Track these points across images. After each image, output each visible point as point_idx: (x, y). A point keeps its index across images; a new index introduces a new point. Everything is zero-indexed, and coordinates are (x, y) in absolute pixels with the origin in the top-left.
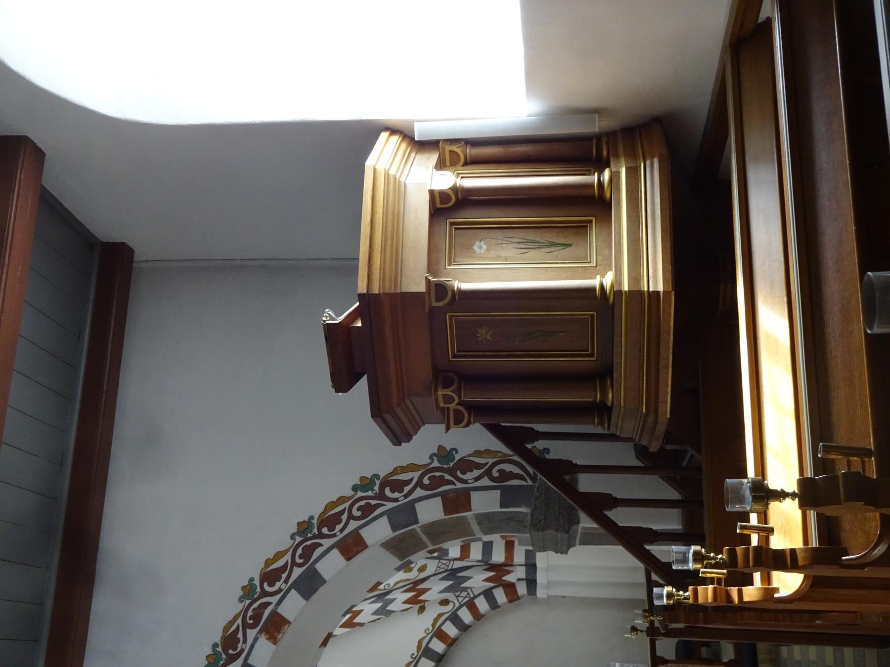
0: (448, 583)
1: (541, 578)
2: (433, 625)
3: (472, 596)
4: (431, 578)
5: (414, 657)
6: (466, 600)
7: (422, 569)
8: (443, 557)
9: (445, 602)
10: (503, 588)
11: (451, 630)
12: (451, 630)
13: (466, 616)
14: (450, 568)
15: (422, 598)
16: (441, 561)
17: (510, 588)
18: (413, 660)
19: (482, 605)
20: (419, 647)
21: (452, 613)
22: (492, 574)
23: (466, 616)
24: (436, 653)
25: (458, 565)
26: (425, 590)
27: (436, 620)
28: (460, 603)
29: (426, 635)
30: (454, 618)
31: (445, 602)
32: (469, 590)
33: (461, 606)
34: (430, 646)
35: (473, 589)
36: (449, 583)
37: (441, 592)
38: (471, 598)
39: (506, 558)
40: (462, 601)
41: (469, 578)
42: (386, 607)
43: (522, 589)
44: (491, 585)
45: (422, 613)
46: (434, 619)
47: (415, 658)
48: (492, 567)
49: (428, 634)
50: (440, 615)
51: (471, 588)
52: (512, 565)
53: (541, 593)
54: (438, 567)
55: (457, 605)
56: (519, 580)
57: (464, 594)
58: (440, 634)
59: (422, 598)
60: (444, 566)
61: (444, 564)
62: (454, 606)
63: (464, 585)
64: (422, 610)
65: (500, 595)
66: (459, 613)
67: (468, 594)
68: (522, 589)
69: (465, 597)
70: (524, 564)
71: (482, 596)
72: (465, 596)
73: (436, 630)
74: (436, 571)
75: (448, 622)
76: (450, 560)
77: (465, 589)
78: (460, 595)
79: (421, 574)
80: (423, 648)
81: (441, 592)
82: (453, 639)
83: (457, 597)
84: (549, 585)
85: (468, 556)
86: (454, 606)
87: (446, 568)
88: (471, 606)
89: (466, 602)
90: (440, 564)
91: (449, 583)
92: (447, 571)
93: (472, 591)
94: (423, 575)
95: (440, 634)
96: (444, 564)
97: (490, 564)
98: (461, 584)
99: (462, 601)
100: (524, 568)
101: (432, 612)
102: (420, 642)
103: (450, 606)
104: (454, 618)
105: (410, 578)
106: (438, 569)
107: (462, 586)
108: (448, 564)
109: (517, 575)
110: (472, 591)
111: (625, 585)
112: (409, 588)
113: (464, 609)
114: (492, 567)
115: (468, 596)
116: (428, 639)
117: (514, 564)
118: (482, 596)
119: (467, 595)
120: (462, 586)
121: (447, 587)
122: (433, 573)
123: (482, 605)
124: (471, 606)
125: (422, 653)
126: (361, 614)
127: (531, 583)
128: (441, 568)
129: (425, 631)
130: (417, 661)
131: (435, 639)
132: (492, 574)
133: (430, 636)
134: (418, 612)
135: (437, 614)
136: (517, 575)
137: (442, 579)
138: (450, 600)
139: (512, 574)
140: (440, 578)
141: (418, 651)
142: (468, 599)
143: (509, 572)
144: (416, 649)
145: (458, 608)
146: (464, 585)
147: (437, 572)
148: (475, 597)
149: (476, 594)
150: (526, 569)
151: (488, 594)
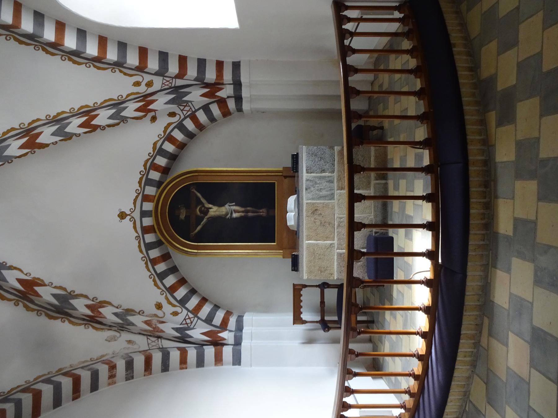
0: (172, 96)
1: (245, 93)
2: (165, 132)
3: (194, 110)
4: (158, 93)
5: (150, 155)
6: (189, 113)
7: (149, 84)
8: (183, 104)
9: (172, 114)
10: (217, 103)
11: (179, 136)
12: (179, 136)
13: (190, 125)
14: (173, 85)
15: (151, 107)
16: (164, 78)
17: (222, 102)
18: (150, 157)
19: (202, 117)
20: (154, 148)
21: (179, 122)
22: (207, 90)
23: (190, 125)
24: (168, 152)
25: (179, 82)
26: (153, 102)
27: (166, 128)
28: (184, 116)
29: (159, 139)
30: (181, 127)
31: (172, 114)
32: (190, 104)
33: (185, 118)
34: (163, 147)
35: (192, 103)
36: (172, 96)
37: (166, 103)
38: (193, 111)
39: (217, 76)
40: (186, 115)
41: (189, 93)
42: (121, 113)
43: (231, 104)
44: (206, 100)
45: (154, 122)
46: (164, 127)
47: (152, 156)
48: (207, 85)
49: (161, 138)
50: (169, 125)
51: (191, 102)
52: (223, 84)
53: (246, 106)
54: (163, 84)
55: (182, 117)
56: (228, 97)
57: (187, 108)
58: (170, 139)
59: (151, 107)
60: (168, 83)
61: (168, 81)
62: (180, 117)
63: (184, 99)
64: (154, 119)
65: (215, 110)
66: (184, 123)
67: (191, 108)
68: (231, 104)
69: (189, 111)
70: (232, 82)
71: (201, 110)
72: (188, 110)
73: (167, 135)
74: (162, 87)
75: (176, 130)
76: (172, 78)
77: (187, 102)
78: (184, 109)
79: (149, 88)
80: (157, 148)
81: (166, 103)
82: (181, 142)
83: (182, 110)
84: (251, 100)
85: (185, 74)
86: (180, 117)
87: (170, 85)
88: (193, 118)
89: (190, 114)
90: (164, 81)
91: (172, 96)
92: (171, 88)
93: (192, 104)
94: (151, 90)
95: (170, 139)
96: (168, 81)
97: (206, 83)
98: (183, 98)
99: (186, 115)
100: (232, 86)
101: (163, 121)
102: (155, 144)
103: (177, 117)
104: (181, 127)
105: (140, 92)
106: (163, 85)
107: (183, 99)
108: (171, 81)
109: (227, 92)
110: (192, 104)
111: (308, 97)
112: (140, 100)
113: (188, 119)
114: (207, 85)
115: (191, 110)
116: (162, 142)
117: (225, 83)
118: (201, 110)
119: (190, 110)
120: (183, 99)
121: (171, 99)
122: (159, 89)
123: (202, 117)
124: (193, 118)
125: (157, 152)
126: (98, 116)
127: (238, 99)
128: (166, 85)
129: (158, 136)
130: (153, 158)
131: (166, 142)
132: (207, 90)
133: (163, 139)
134: (151, 120)
135: (167, 123)
136: (227, 92)
137: (167, 94)
138: (177, 113)
139: (223, 90)
140: (165, 93)
141: (154, 151)
142: (191, 112)
143: (221, 89)
144: (152, 150)
145: (183, 119)
146: (184, 99)
147: (162, 88)
148: (196, 111)
149: (196, 109)
150: (234, 87)
151: (206, 108)
